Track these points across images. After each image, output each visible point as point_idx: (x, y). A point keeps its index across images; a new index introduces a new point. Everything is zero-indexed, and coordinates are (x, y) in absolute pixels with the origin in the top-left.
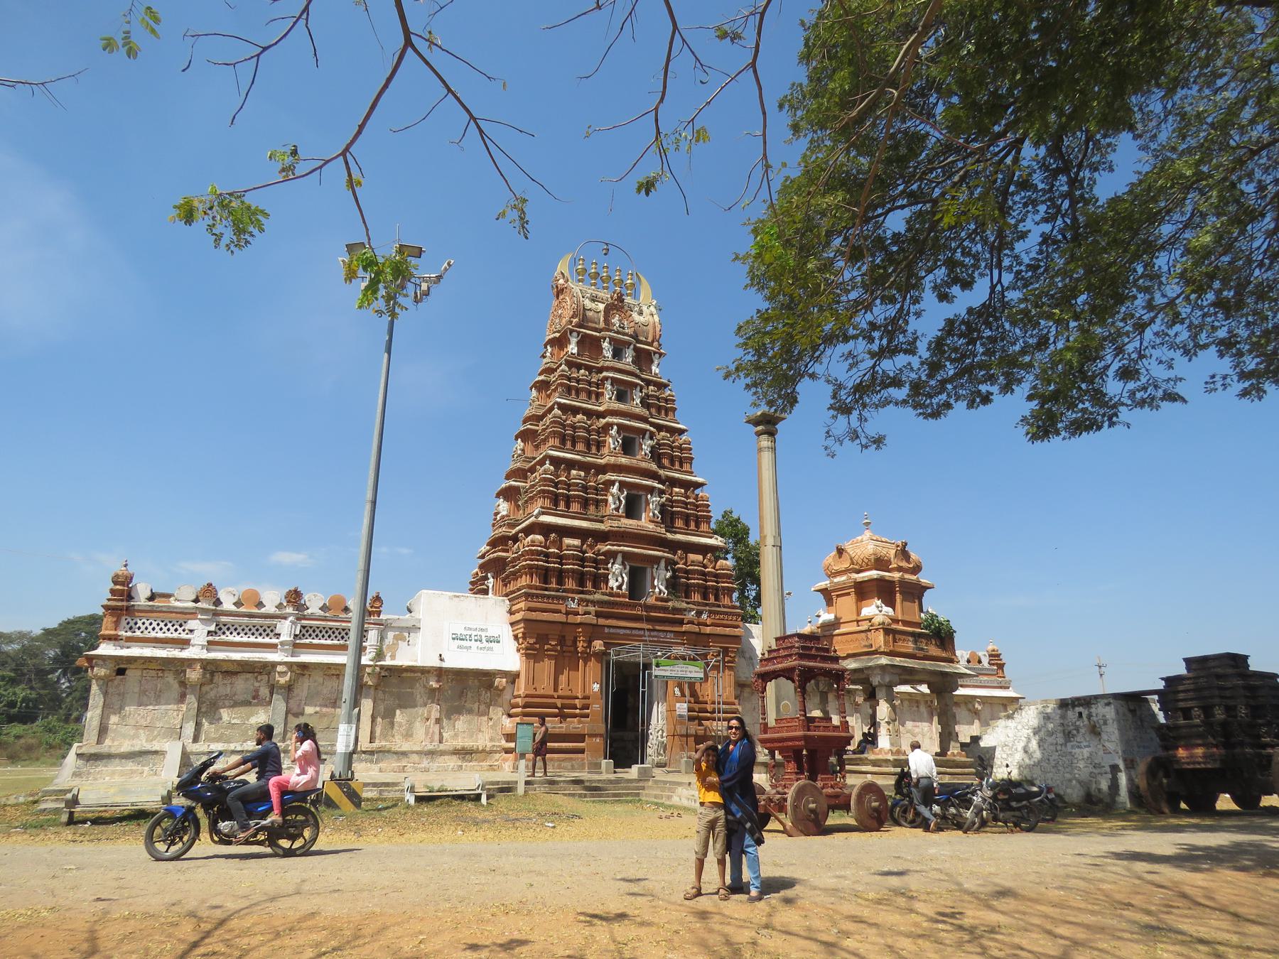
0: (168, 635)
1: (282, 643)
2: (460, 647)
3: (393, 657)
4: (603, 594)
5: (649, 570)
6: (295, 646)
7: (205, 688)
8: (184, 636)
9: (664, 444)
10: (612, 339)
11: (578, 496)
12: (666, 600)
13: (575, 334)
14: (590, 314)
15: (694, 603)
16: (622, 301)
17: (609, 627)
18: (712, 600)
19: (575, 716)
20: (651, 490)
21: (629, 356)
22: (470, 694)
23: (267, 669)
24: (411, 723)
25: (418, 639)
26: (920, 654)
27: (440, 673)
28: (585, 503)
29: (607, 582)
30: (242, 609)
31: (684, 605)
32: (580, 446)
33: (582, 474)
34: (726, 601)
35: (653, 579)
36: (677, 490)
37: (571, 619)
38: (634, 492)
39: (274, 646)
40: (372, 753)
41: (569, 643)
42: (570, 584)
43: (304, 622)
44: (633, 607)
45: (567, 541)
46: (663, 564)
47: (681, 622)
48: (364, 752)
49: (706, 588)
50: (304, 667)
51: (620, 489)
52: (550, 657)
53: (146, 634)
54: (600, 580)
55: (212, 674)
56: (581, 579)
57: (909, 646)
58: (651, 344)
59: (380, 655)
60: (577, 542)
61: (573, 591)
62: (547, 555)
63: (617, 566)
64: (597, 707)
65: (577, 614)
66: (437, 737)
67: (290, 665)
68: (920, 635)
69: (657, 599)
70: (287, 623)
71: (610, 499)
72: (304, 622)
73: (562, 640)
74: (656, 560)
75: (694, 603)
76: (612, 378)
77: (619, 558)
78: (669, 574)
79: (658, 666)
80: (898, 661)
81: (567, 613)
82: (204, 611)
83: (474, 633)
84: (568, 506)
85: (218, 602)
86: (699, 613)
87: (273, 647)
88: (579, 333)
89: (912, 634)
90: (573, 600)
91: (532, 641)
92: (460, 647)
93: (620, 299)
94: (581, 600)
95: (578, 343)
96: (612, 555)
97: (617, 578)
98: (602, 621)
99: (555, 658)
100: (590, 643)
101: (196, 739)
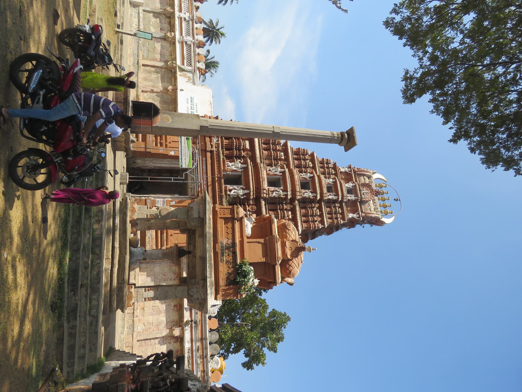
0: (183, 8)
1: (183, 37)
2: (187, 99)
3: (180, 75)
4: (223, 158)
6: (182, 43)
7: (164, 16)
8: (183, 12)
9: (313, 211)
10: (355, 186)
11: (271, 153)
12: (226, 194)
13: (350, 169)
14: (362, 178)
16: (377, 196)
17: (206, 160)
19: (156, 139)
20: (285, 190)
21: (352, 197)
22: (165, 106)
23: (172, 29)
24: (151, 81)
25: (190, 85)
26: (219, 246)
27: (175, 90)
28: (269, 157)
29: (230, 162)
30: (195, 29)
32: (296, 162)
33: (283, 158)
38: (281, 182)
39: (181, 34)
40: (138, 64)
42: (226, 142)
43: (192, 45)
45: (247, 143)
46: (246, 191)
48: (138, 61)
50: (174, 43)
53: (182, 3)
54: (230, 158)
55: (169, 18)
56: (229, 148)
57: (224, 240)
58: (362, 212)
59: (182, 70)
60: (248, 146)
61: (222, 142)
64: (161, 150)
65: (211, 141)
66: (144, 89)
67: (174, 38)
68: (234, 253)
70: (191, 39)
72: (192, 45)
74: (247, 187)
76: (336, 181)
77: (244, 166)
79: (187, 139)
80: (209, 216)
82: (193, 17)
83: (195, 107)
84: (265, 149)
85: (196, 23)
87: (181, 34)
88: (351, 171)
89: (234, 244)
90: (218, 141)
92: (187, 99)
93: (377, 193)
94: (218, 144)
95: (346, 172)
96: (245, 163)
97: (235, 166)
98: (209, 154)
101: (144, 11)
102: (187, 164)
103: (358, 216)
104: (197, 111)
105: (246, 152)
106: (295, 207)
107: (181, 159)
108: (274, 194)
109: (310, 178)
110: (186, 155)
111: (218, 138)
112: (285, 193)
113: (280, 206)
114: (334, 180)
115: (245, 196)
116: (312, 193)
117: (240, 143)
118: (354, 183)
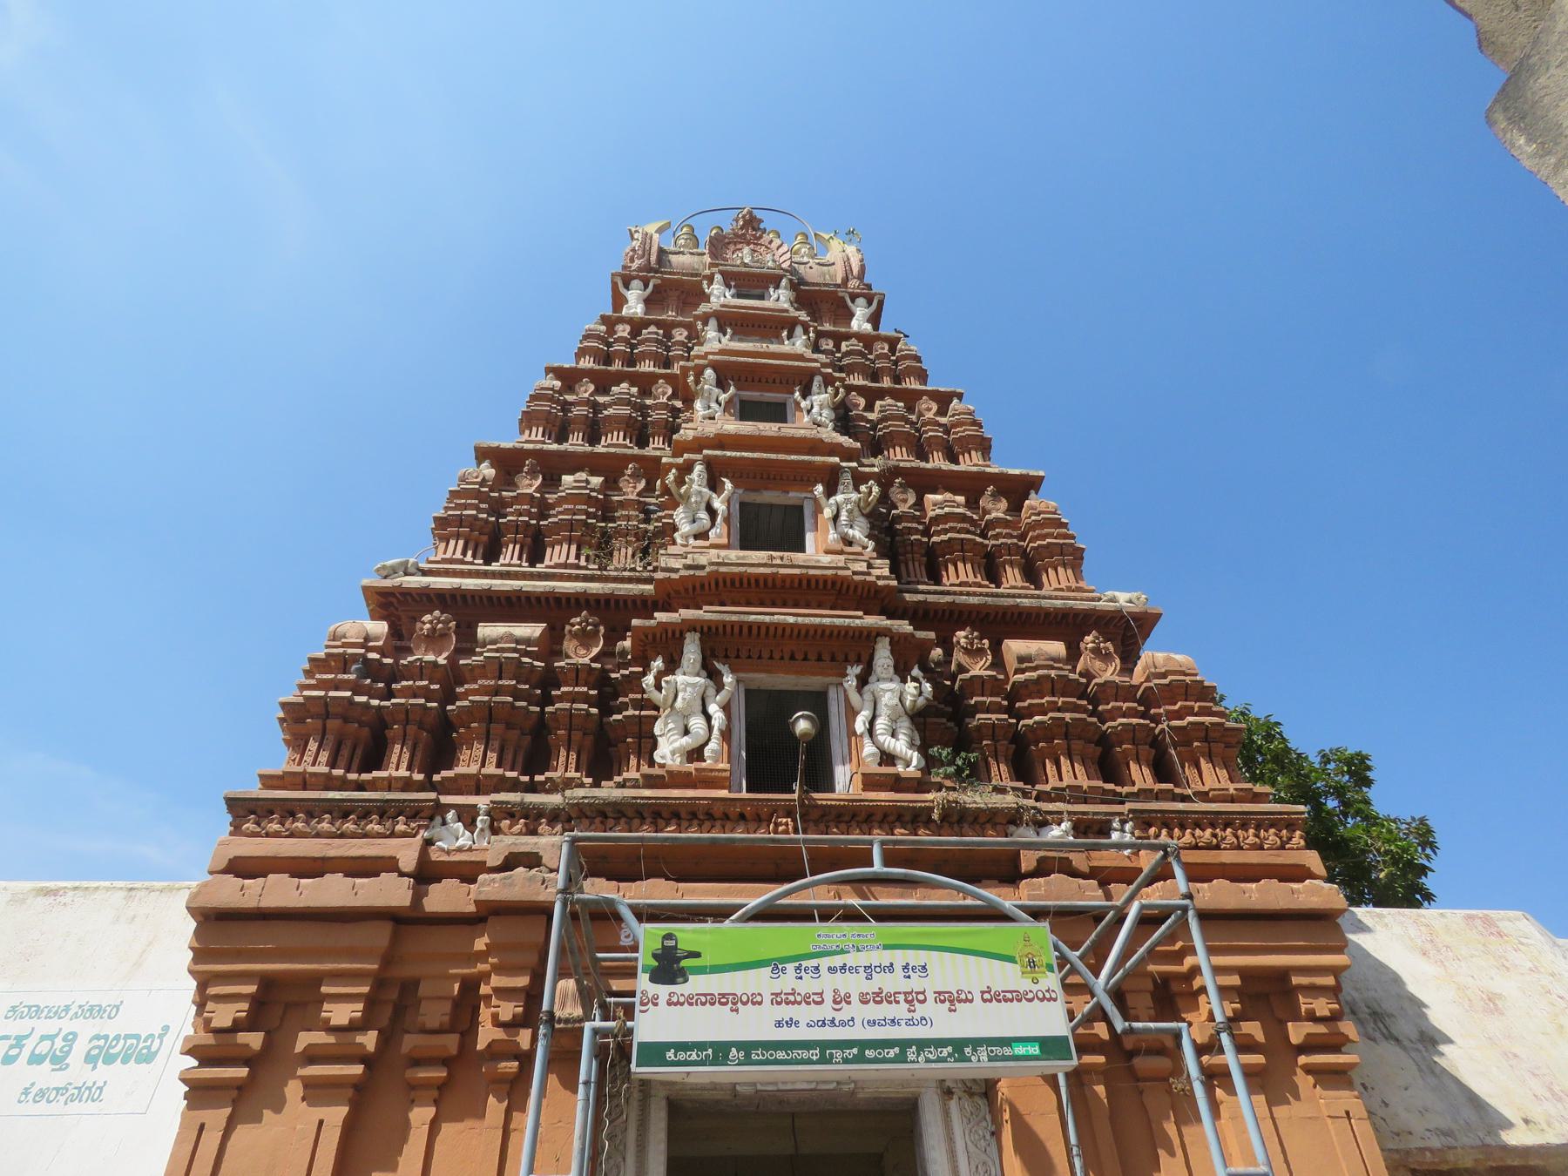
5: (832, 693)
12: (920, 786)
13: (636, 283)
15: (1058, 795)
18: (1141, 776)
21: (780, 299)
31: (1009, 800)
34: (1213, 777)
35: (852, 713)
36: (939, 497)
37: (445, 897)
38: (769, 497)
41: (434, 1013)
44: (760, 818)
46: (883, 657)
47: (1007, 872)
49: (1105, 742)
51: (714, 485)
52: (317, 1091)
54: (613, 742)
60: (532, 630)
61: (478, 785)
62: (394, 675)
63: (679, 678)
69: (870, 782)
71: (680, 515)
73: (392, 1002)
75: (1058, 795)
77: (692, 652)
78: (916, 691)
79: (669, 967)
81: (426, 874)
84: (536, 556)
86: (1091, 829)
90: (468, 816)
91: (224, 1016)
94: (499, 814)
97: (691, 720)
99: (360, 1096)
100: (532, 996)
102: (1008, 976)
103: (861, 301)
104: (94, 1011)
105: (569, 645)
106: (896, 471)
107: (959, 1046)
108: (857, 533)
109: (721, 384)
110: (892, 983)
111: (440, 809)
112: (847, 479)
113: (910, 531)
114: (713, 323)
115: (916, 672)
116: (806, 394)
117: (500, 668)
118: (711, 279)
